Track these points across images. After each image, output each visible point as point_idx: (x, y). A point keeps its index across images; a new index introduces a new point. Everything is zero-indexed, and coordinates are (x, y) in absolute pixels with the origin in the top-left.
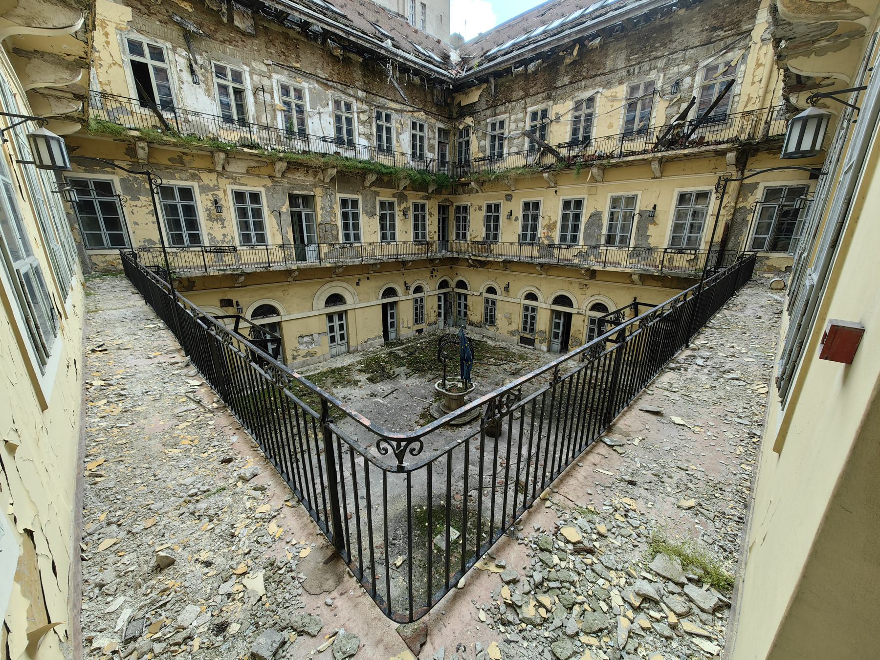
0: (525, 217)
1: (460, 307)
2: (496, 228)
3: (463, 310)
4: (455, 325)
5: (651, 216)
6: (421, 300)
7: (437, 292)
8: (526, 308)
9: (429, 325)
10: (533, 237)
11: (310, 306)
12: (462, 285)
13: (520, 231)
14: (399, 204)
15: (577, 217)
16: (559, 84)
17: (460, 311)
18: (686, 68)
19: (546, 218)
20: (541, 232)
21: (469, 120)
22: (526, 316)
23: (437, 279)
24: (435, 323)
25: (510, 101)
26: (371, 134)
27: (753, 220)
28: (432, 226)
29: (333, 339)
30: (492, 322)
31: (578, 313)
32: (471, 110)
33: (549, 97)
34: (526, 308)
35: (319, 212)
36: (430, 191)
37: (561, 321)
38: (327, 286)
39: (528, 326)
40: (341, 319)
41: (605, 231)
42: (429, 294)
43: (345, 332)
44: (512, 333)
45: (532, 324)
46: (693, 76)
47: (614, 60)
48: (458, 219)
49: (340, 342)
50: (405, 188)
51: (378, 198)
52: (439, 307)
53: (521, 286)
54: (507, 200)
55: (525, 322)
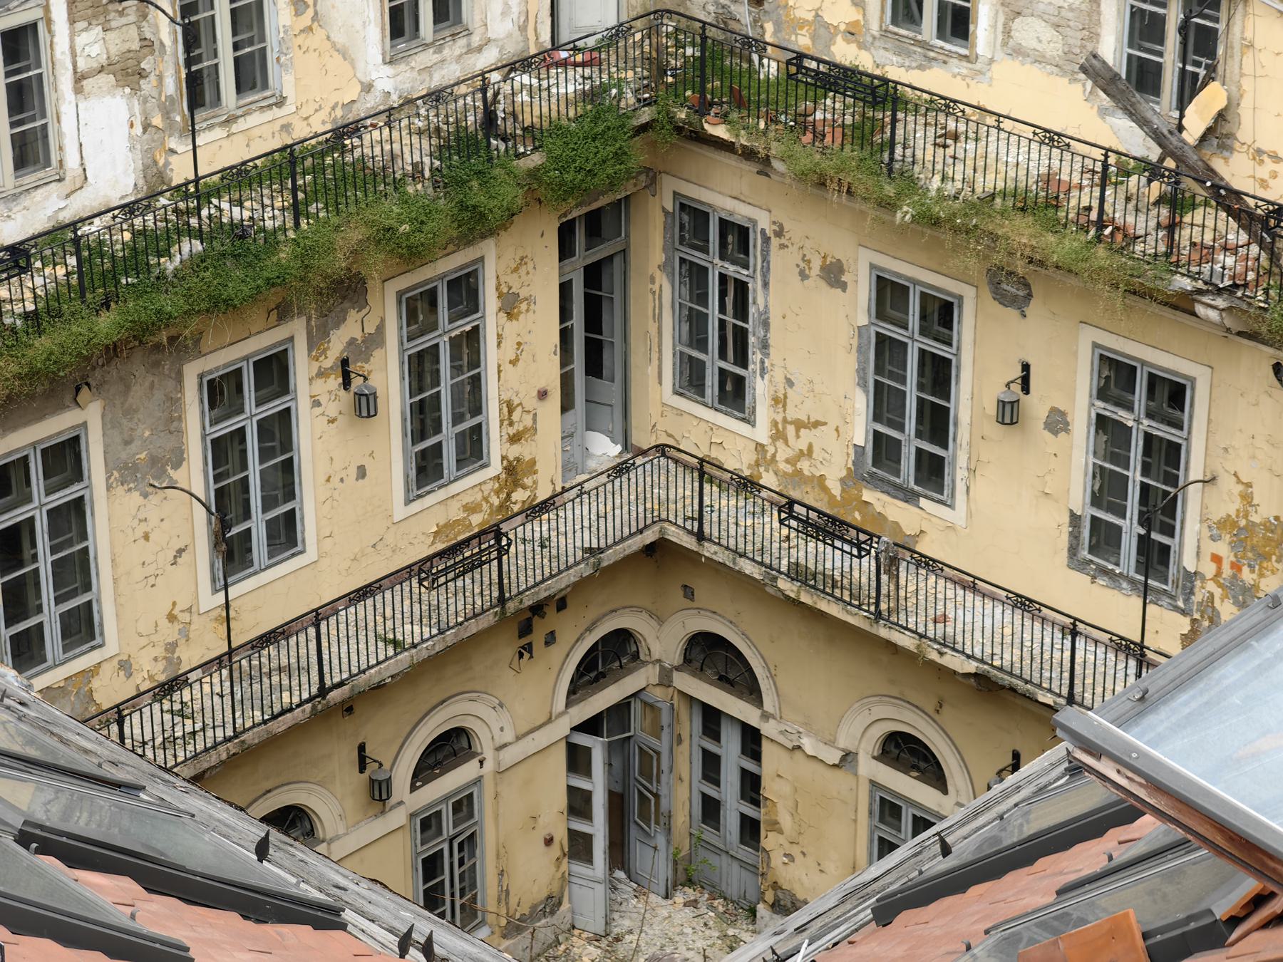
2: (936, 423)
3: (733, 807)
4: (685, 877)
6: (464, 805)
7: (562, 728)
10: (1154, 558)
13: (1077, 495)
14: (317, 341)
17: (711, 810)
20: (1194, 545)
23: (557, 651)
24: (552, 904)
26: (148, 45)
28: (522, 349)
42: (509, 756)
48: (695, 276)
52: (579, 804)
54: (1004, 299)
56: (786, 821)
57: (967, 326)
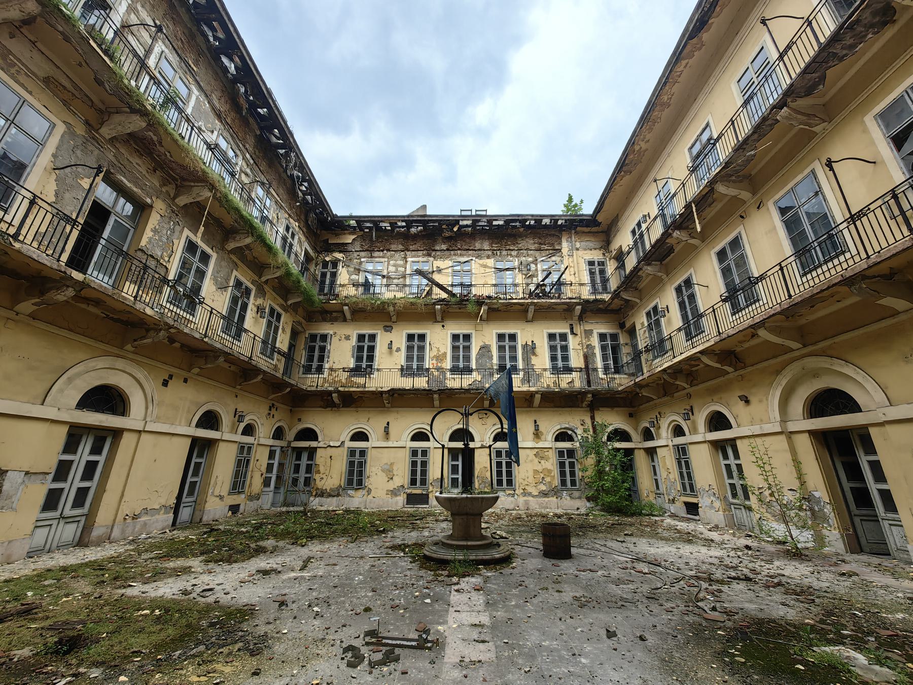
0: (410, 348)
1: (297, 469)
5: (531, 350)
8: (414, 453)
9: (251, 498)
11: (40, 389)
12: (310, 434)
15: (467, 349)
16: (437, 248)
18: (530, 259)
19: (434, 349)
21: (339, 256)
22: (414, 464)
25: (388, 250)
27: (598, 352)
29: (52, 501)
30: (360, 483)
31: (483, 447)
32: (342, 248)
33: (429, 255)
34: (414, 453)
35: (148, 233)
36: (289, 302)
37: (460, 463)
38: (101, 363)
39: (418, 477)
40: (96, 450)
41: (495, 361)
43: (93, 484)
44: (394, 493)
45: (424, 473)
46: (536, 265)
47: (482, 244)
49: (68, 512)
50: (266, 282)
51: (235, 273)
53: (405, 424)
54: (386, 331)
55: (414, 473)
56: (322, 469)
57: (378, 339)
